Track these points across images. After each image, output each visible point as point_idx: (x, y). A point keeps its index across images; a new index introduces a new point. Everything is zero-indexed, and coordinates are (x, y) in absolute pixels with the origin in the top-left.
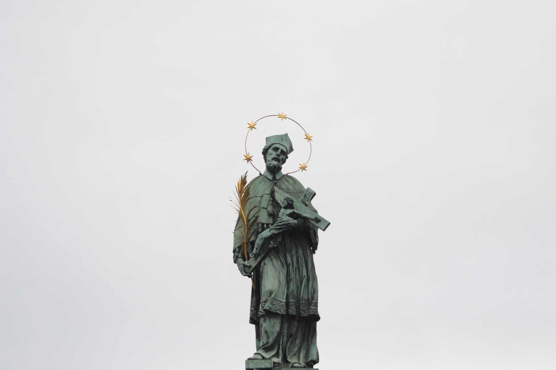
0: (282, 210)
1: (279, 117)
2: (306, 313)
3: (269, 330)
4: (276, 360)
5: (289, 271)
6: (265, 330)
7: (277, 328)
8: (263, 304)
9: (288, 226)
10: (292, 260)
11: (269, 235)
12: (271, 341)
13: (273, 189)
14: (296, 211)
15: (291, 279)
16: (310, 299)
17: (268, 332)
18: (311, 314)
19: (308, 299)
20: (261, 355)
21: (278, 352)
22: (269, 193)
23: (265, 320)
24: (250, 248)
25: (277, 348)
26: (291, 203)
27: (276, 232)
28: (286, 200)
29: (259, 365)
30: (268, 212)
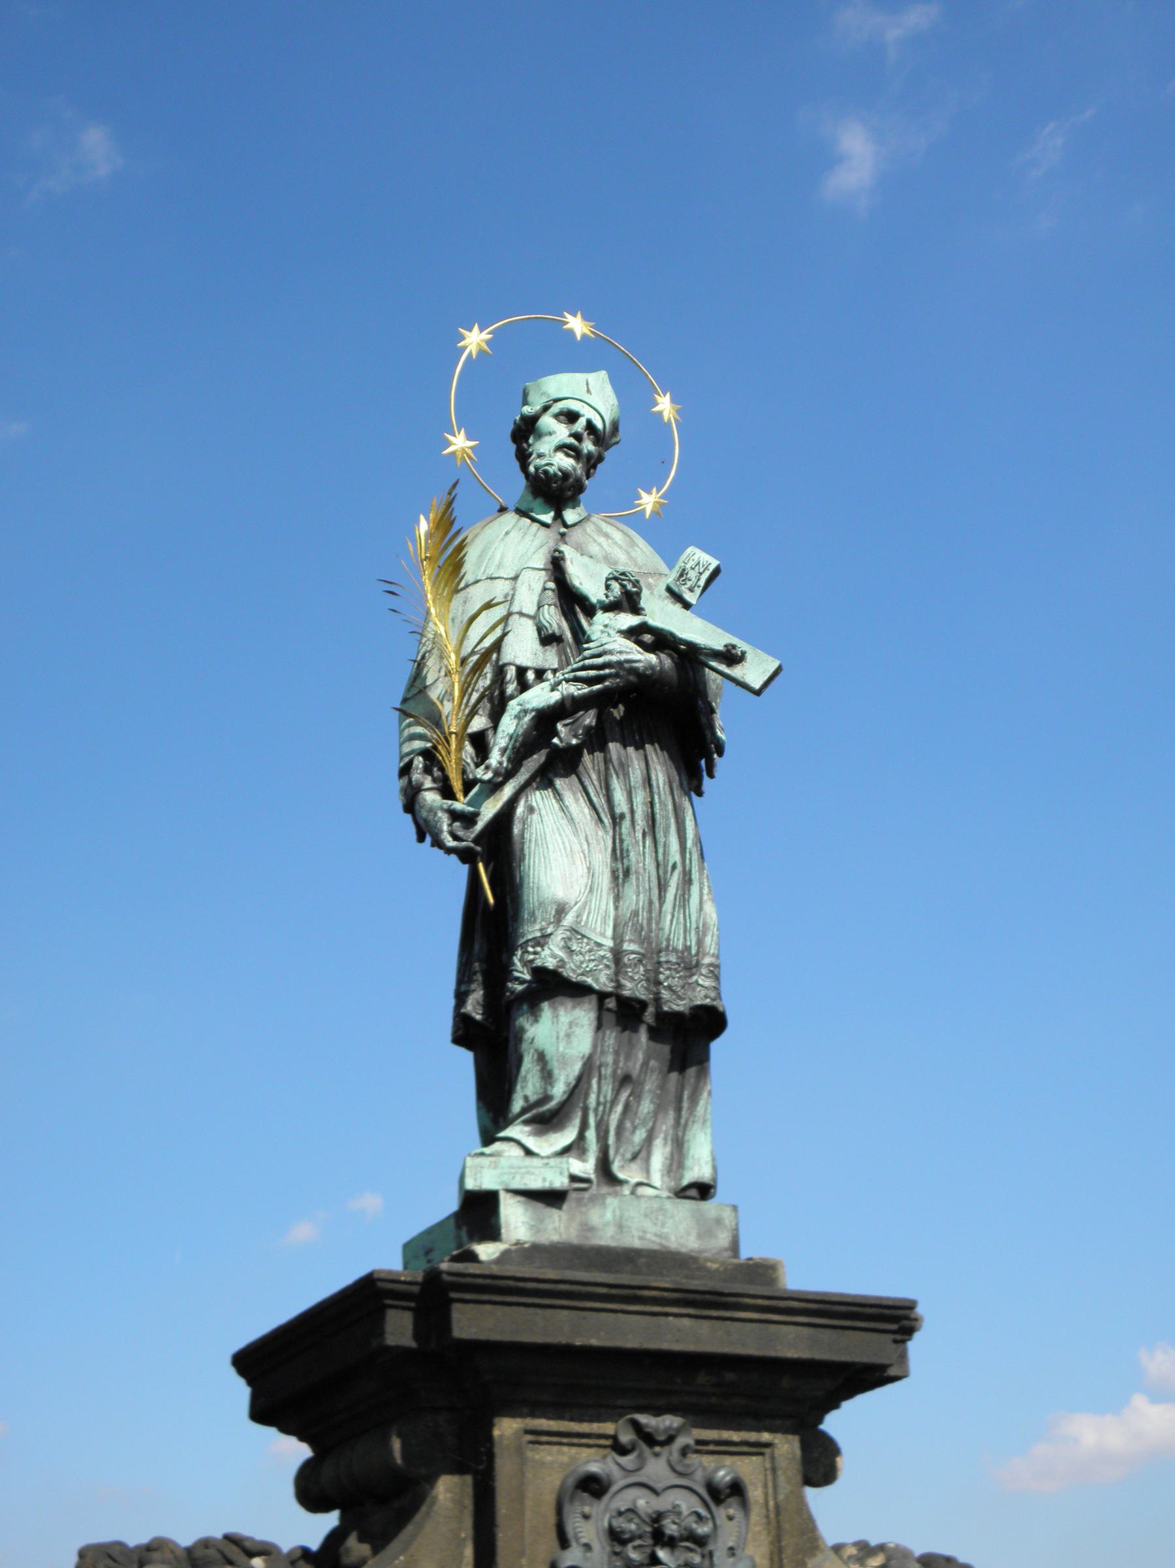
0: (601, 617)
2: (681, 999)
3: (550, 1052)
5: (622, 841)
8: (530, 949)
12: (559, 1090)
13: (556, 550)
14: (652, 622)
17: (548, 1057)
18: (699, 1003)
19: (687, 948)
20: (518, 1143)
21: (581, 1137)
22: (542, 567)
24: (472, 759)
25: (577, 1122)
26: (635, 589)
27: (580, 692)
30: (540, 629)
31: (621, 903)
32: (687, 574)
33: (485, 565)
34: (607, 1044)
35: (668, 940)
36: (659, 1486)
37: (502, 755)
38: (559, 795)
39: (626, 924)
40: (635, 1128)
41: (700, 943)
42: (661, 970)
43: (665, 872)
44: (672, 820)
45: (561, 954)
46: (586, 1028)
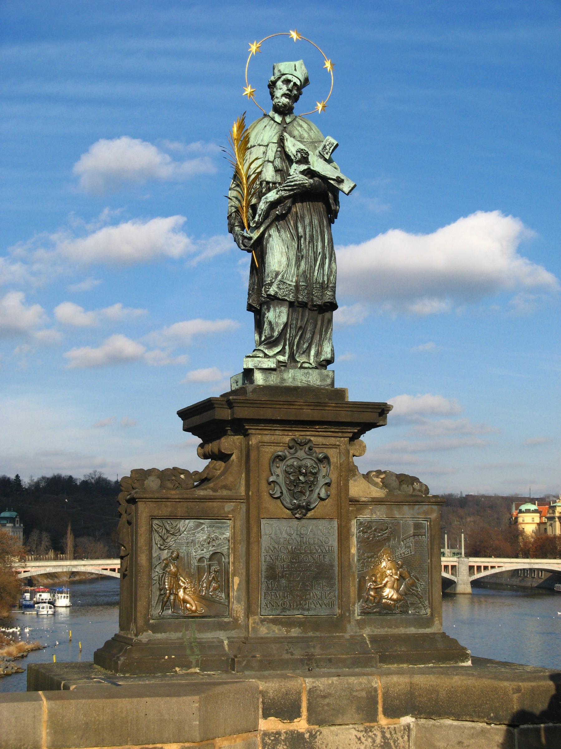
0: (294, 166)
3: (273, 321)
4: (281, 358)
5: (301, 245)
6: (269, 321)
7: (284, 319)
11: (276, 198)
12: (276, 334)
14: (312, 168)
16: (326, 283)
17: (273, 323)
19: (324, 281)
20: (262, 351)
21: (284, 348)
25: (282, 344)
28: (299, 152)
30: (275, 167)
35: (316, 280)
36: (301, 459)
40: (304, 343)
41: (328, 279)
43: (317, 256)
45: (276, 290)
46: (285, 313)
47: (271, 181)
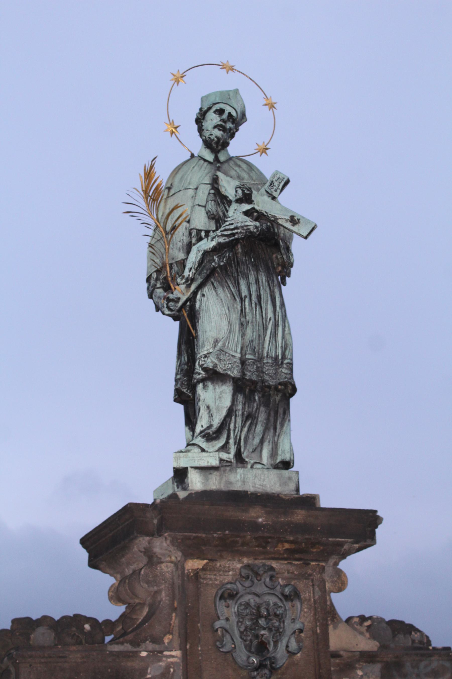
0: (234, 206)
1: (221, 67)
2: (274, 379)
3: (212, 405)
4: (224, 456)
5: (245, 308)
7: (227, 402)
8: (203, 359)
9: (244, 230)
10: (249, 290)
12: (216, 423)
14: (257, 208)
15: (248, 322)
16: (280, 357)
17: (211, 408)
18: (282, 381)
19: (277, 357)
21: (227, 442)
22: (208, 183)
23: (205, 387)
25: (225, 436)
26: (248, 192)
27: (224, 241)
29: (198, 462)
30: (208, 212)
31: (245, 337)
32: (274, 183)
33: (183, 183)
34: (239, 401)
37: (190, 271)
38: (216, 288)
39: (247, 346)
40: (254, 438)
42: (265, 366)
44: (269, 298)
45: (216, 361)
46: (228, 394)
47: (202, 228)
